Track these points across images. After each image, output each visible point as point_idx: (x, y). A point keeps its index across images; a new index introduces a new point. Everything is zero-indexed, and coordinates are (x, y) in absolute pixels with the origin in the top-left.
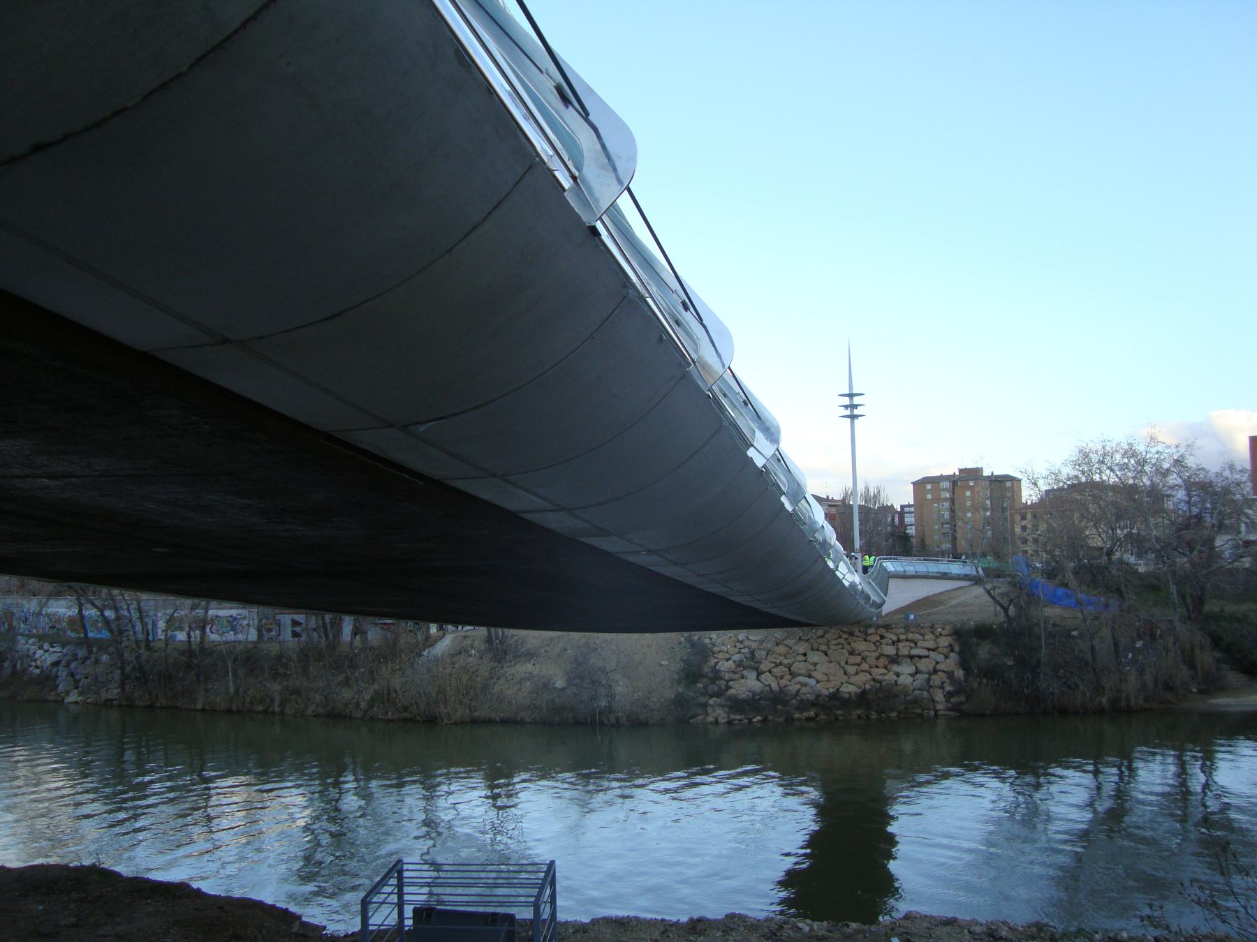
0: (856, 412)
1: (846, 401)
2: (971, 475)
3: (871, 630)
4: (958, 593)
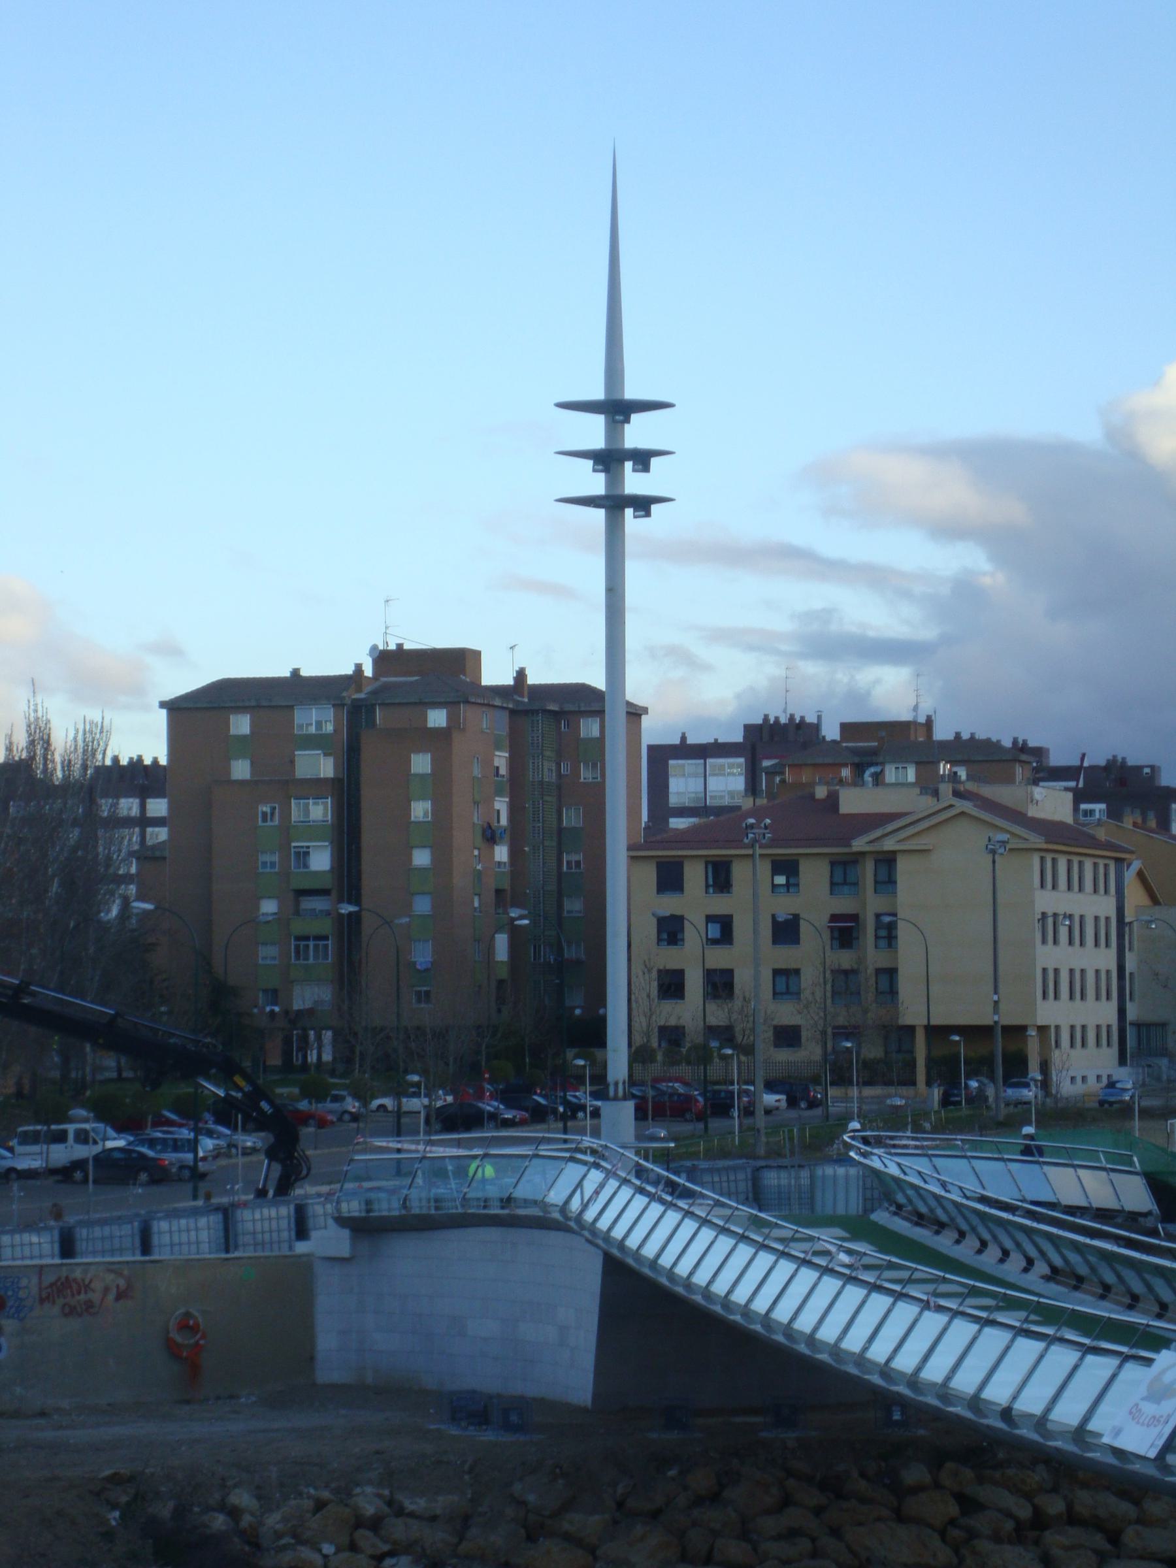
0: (634, 483)
1: (592, 432)
3: (915, 1474)
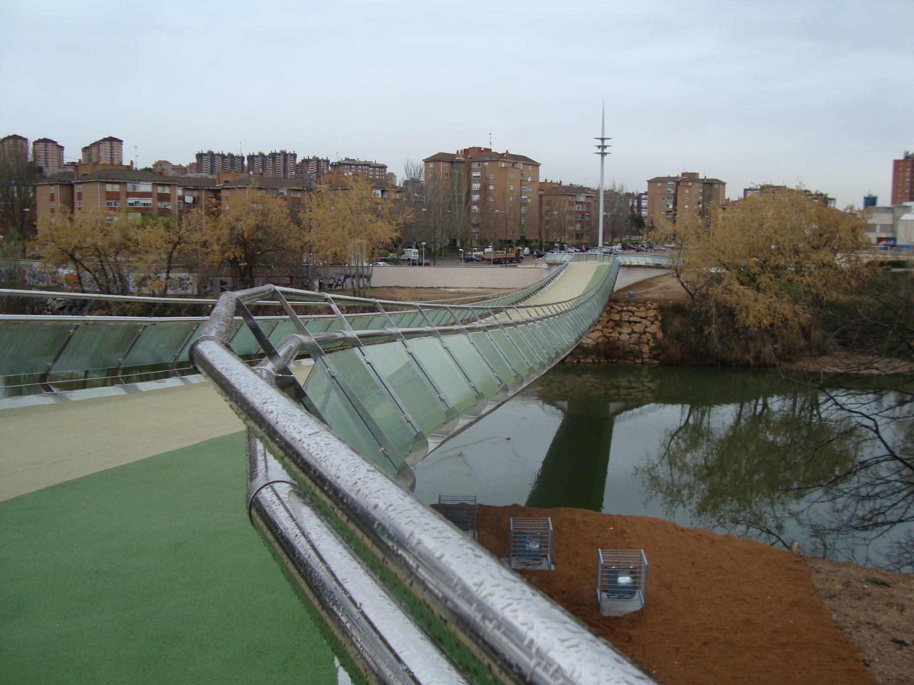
0: (605, 151)
1: (599, 143)
2: (691, 177)
4: (666, 278)
